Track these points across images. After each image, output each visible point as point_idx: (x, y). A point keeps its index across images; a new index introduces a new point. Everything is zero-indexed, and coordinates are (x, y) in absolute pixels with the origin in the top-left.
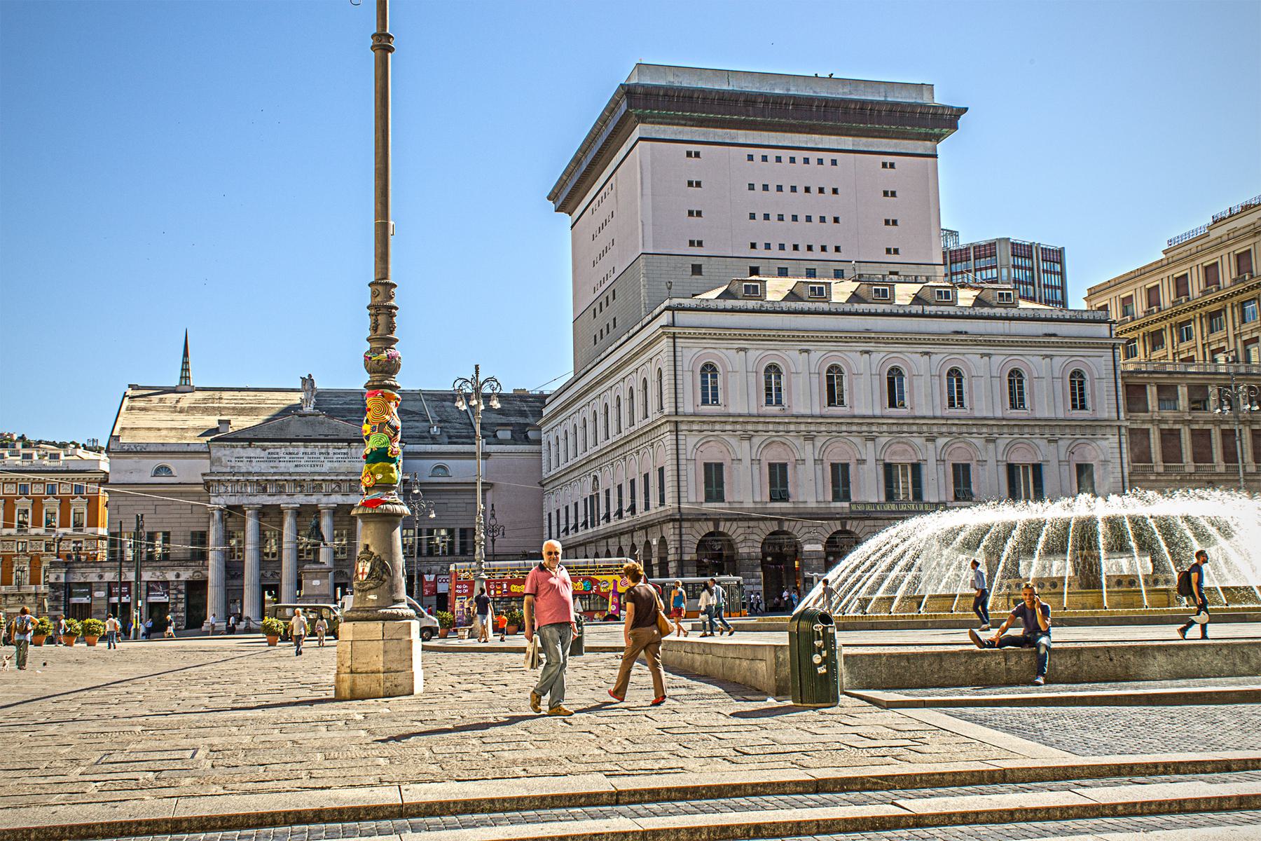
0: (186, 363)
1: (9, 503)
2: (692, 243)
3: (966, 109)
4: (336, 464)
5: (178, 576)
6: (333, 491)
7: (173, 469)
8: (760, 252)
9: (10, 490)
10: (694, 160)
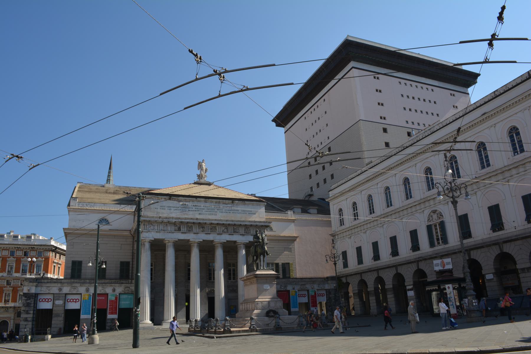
0: (109, 172)
1: (4, 260)
2: (381, 118)
3: (479, 75)
4: (224, 214)
5: (114, 290)
6: (223, 231)
7: (110, 221)
8: (410, 125)
9: (5, 253)
10: (376, 80)
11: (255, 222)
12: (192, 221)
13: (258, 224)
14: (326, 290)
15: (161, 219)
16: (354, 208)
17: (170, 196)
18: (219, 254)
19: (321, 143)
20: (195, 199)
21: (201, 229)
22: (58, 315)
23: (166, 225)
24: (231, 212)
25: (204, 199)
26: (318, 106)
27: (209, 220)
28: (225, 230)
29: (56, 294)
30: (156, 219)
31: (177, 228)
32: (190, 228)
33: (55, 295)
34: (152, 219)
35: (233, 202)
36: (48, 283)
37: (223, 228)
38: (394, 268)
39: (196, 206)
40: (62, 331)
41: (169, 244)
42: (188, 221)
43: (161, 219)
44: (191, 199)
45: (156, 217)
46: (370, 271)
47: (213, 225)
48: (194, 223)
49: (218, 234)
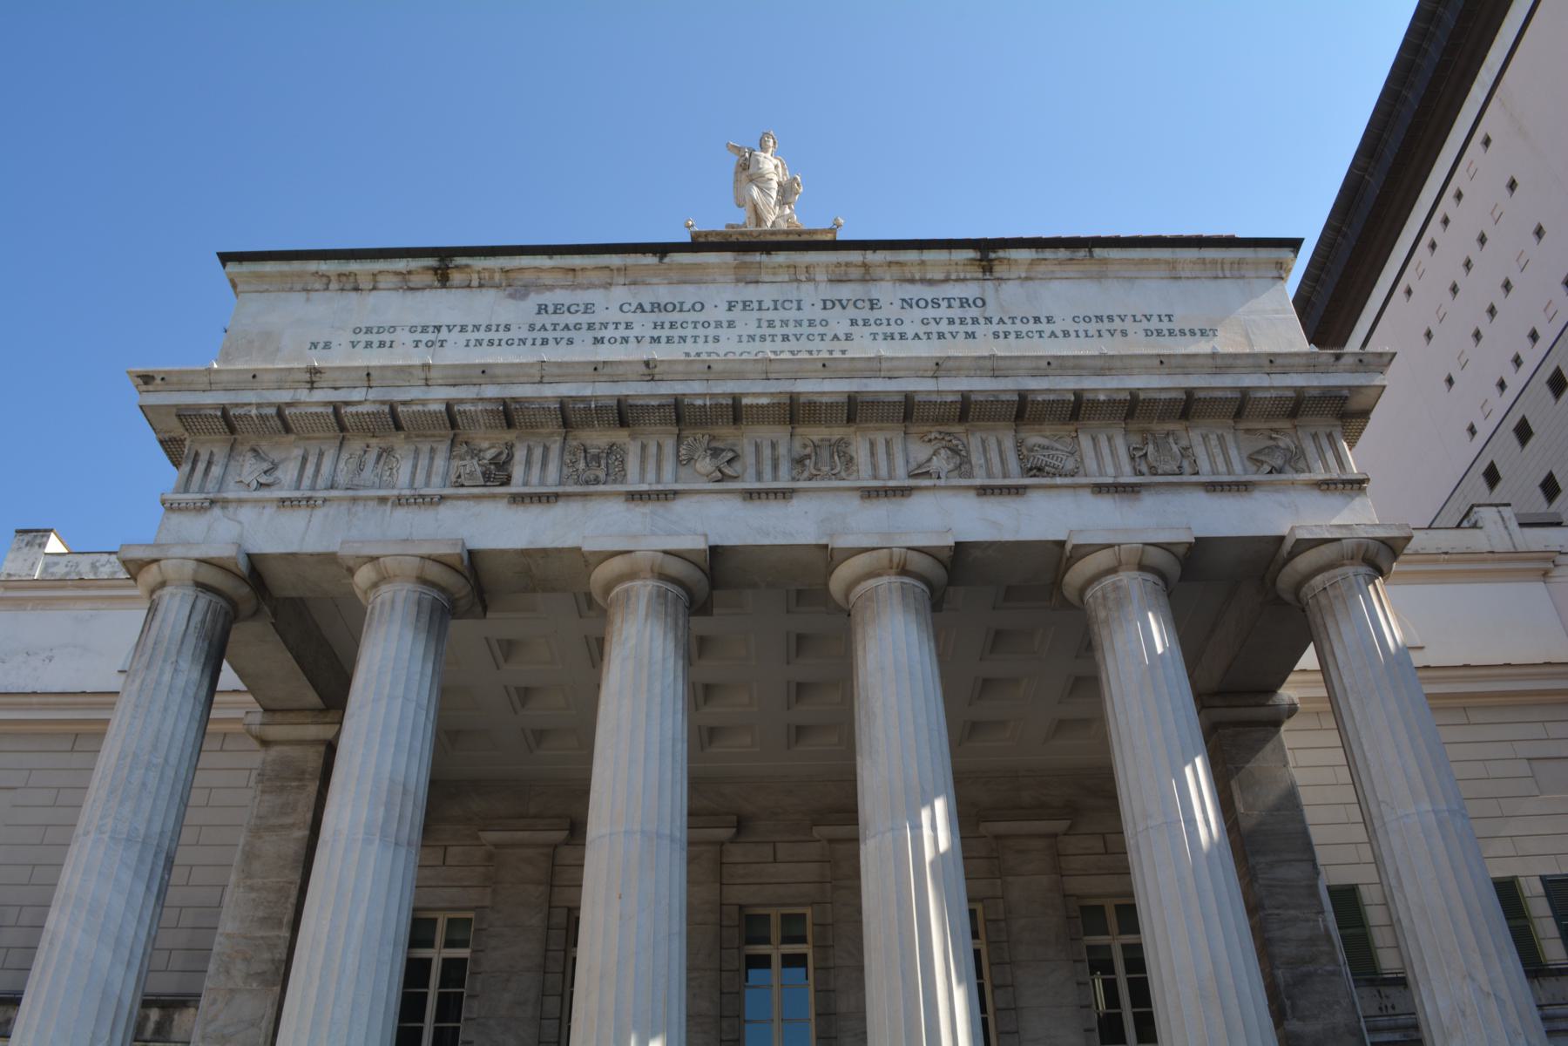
11: (1221, 363)
12: (604, 390)
13: (1248, 381)
15: (319, 395)
17: (444, 263)
18: (896, 673)
19: (1534, 336)
20: (650, 259)
21: (705, 465)
23: (386, 453)
24: (980, 329)
25: (728, 257)
26: (1459, 196)
27: (767, 369)
28: (941, 463)
30: (284, 396)
31: (473, 466)
32: (593, 459)
34: (250, 397)
35: (987, 266)
37: (920, 452)
39: (657, 307)
41: (386, 591)
42: (566, 390)
43: (319, 395)
44: (615, 260)
45: (283, 379)
47: (817, 433)
49: (869, 494)
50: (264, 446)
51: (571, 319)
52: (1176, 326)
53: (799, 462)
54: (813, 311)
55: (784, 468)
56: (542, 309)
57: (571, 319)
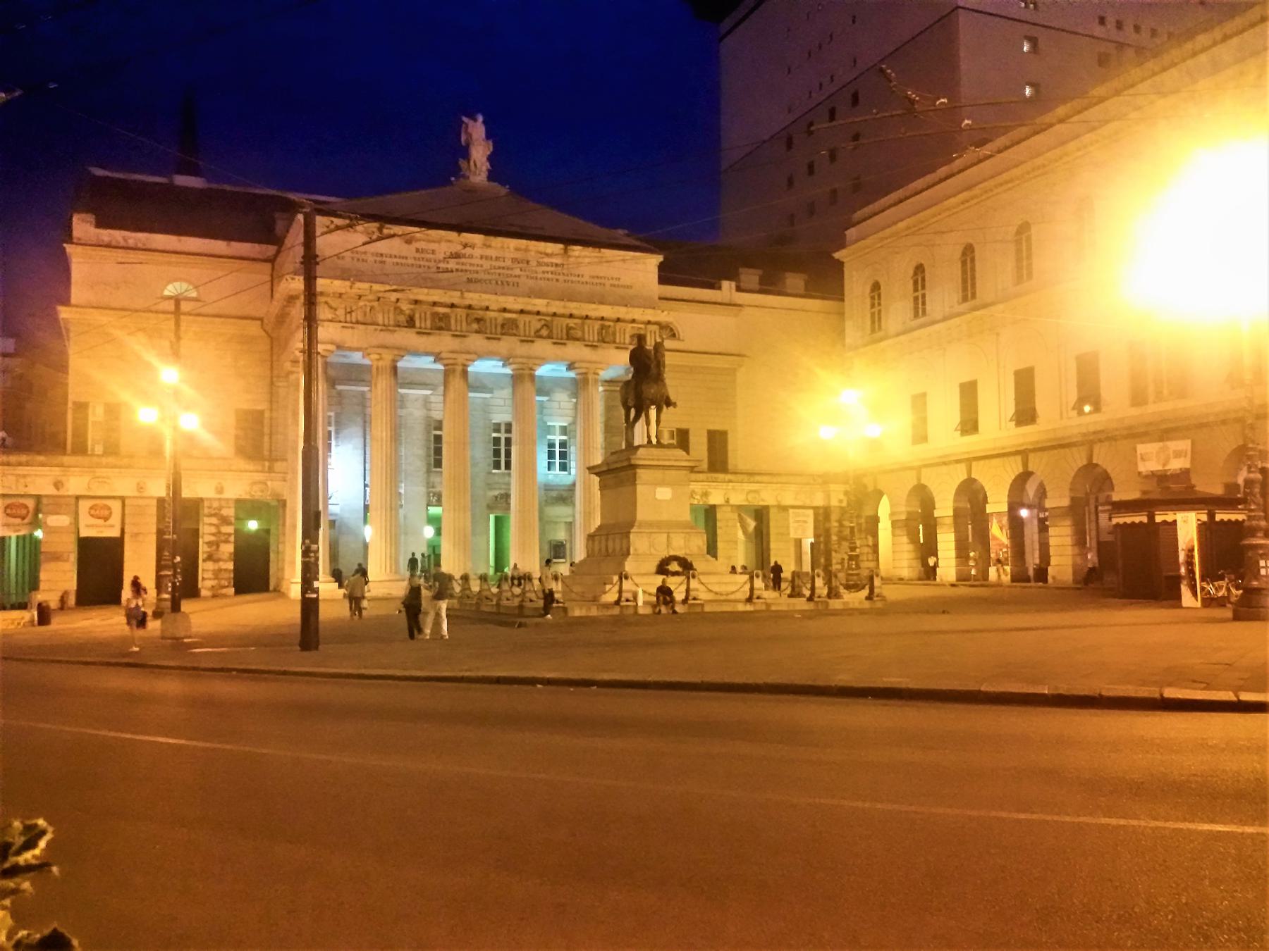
5: (220, 490)
14: (815, 508)
16: (916, 283)
22: (56, 557)
24: (561, 278)
25: (482, 236)
28: (544, 332)
29: (47, 496)
31: (402, 319)
32: (441, 319)
33: (45, 501)
35: (566, 250)
36: (20, 464)
38: (1019, 458)
40: (72, 600)
46: (945, 462)
47: (508, 315)
48: (453, 306)
49: (522, 341)
50: (329, 300)
51: (431, 256)
52: (621, 283)
53: (503, 326)
54: (508, 263)
55: (499, 329)
56: (417, 250)
57: (431, 256)
